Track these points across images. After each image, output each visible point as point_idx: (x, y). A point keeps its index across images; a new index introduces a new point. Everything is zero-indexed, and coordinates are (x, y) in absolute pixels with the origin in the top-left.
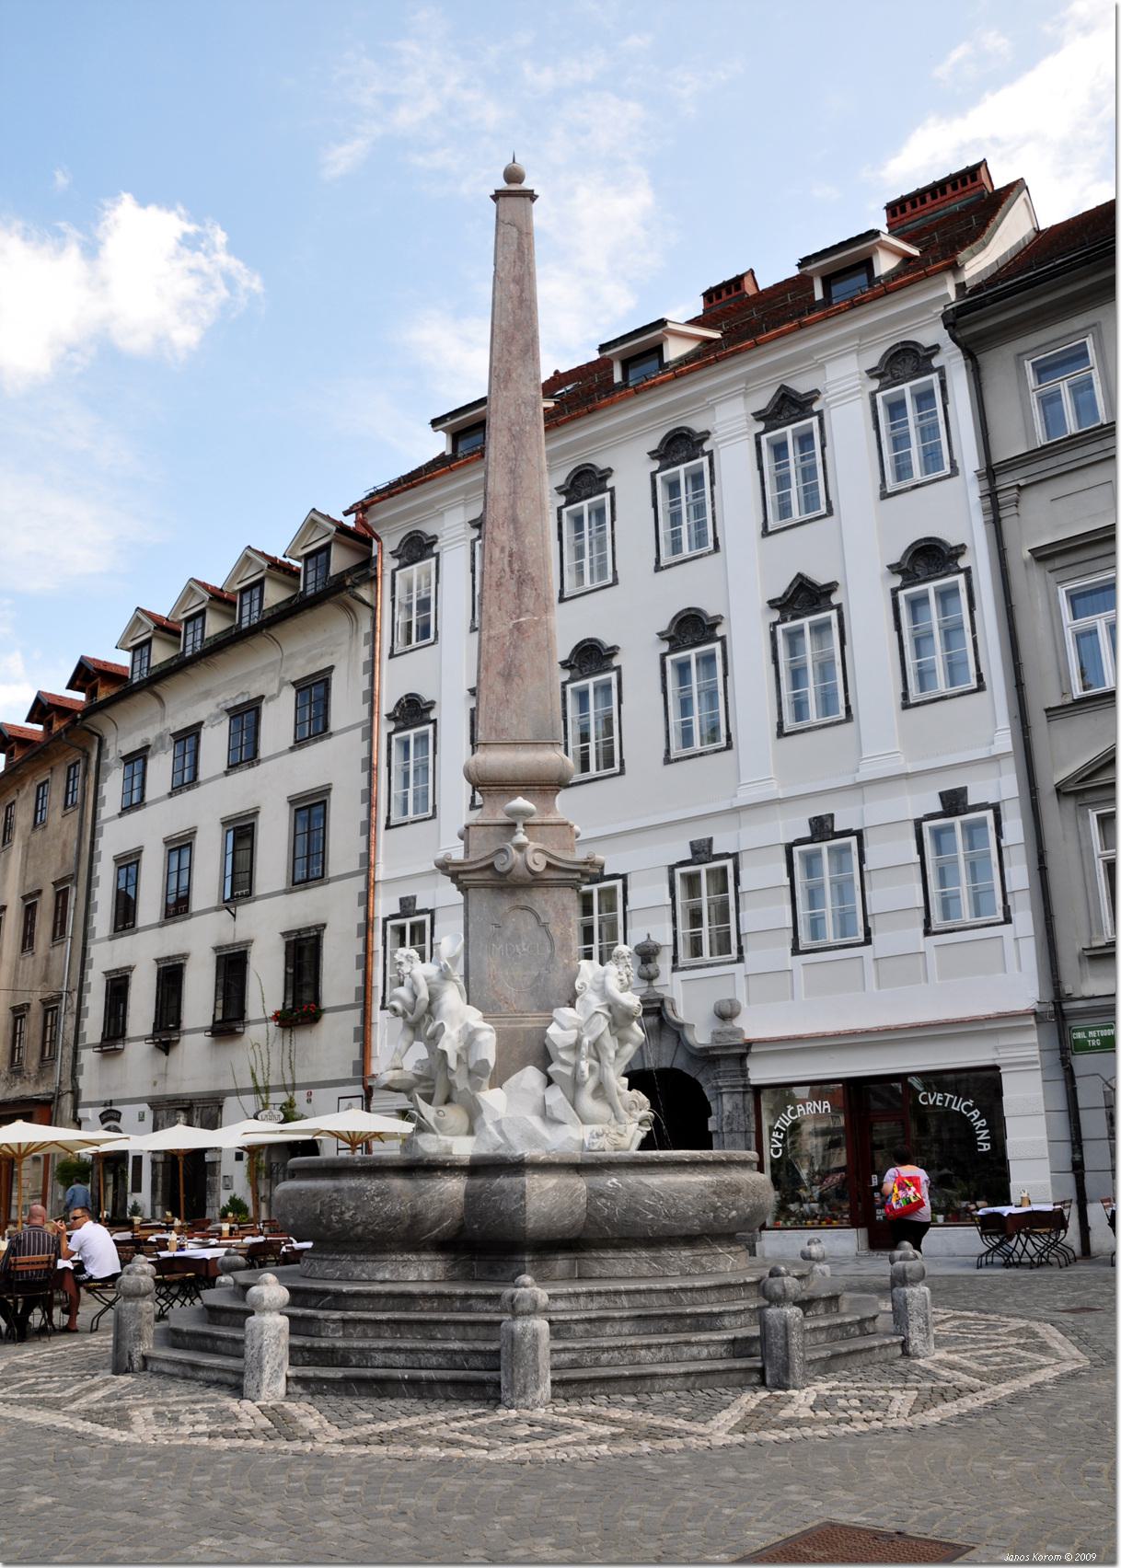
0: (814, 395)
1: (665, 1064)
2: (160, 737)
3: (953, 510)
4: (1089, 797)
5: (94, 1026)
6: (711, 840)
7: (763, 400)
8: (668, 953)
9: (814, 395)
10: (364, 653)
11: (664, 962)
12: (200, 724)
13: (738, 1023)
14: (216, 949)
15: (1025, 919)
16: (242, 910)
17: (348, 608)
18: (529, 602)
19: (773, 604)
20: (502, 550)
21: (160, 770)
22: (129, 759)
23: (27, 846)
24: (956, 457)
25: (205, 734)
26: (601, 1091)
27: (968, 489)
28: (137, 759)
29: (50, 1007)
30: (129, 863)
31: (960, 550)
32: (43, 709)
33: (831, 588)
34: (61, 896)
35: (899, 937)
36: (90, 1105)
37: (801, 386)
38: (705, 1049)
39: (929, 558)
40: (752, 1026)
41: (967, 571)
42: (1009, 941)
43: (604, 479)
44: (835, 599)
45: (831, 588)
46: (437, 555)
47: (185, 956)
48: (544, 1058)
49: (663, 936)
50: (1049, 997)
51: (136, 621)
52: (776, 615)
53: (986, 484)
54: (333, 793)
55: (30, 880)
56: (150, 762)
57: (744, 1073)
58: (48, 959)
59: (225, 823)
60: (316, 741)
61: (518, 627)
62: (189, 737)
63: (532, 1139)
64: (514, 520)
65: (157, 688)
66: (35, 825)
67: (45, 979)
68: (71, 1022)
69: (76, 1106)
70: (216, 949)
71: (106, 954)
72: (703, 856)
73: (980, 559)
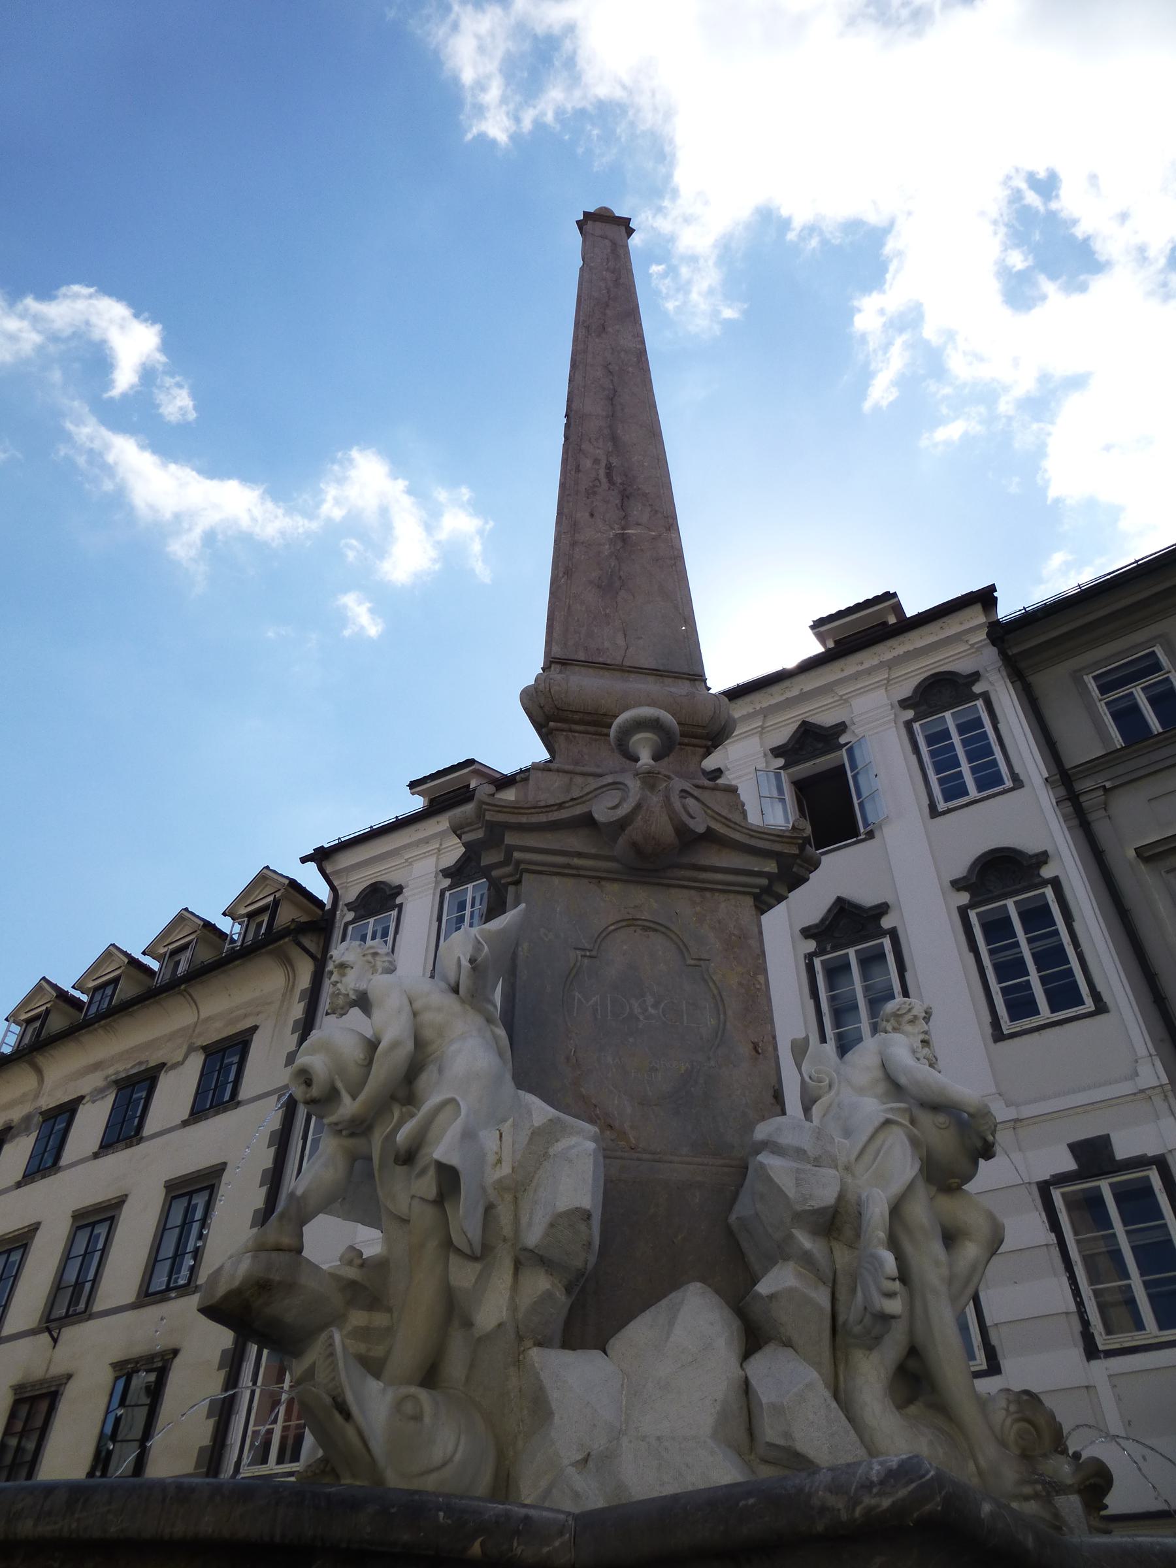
2: (27, 1118)
7: (782, 735)
10: (298, 1010)
12: (82, 1097)
16: (69, 1334)
17: (287, 962)
19: (807, 933)
20: (596, 461)
24: (1017, 770)
31: (1043, 858)
33: (883, 909)
39: (999, 874)
41: (1056, 883)
44: (886, 923)
45: (883, 909)
46: (400, 906)
51: (38, 990)
52: (811, 946)
53: (1062, 792)
54: (226, 1177)
60: (217, 1113)
61: (624, 538)
64: (614, 438)
65: (40, 1060)
73: (1069, 866)
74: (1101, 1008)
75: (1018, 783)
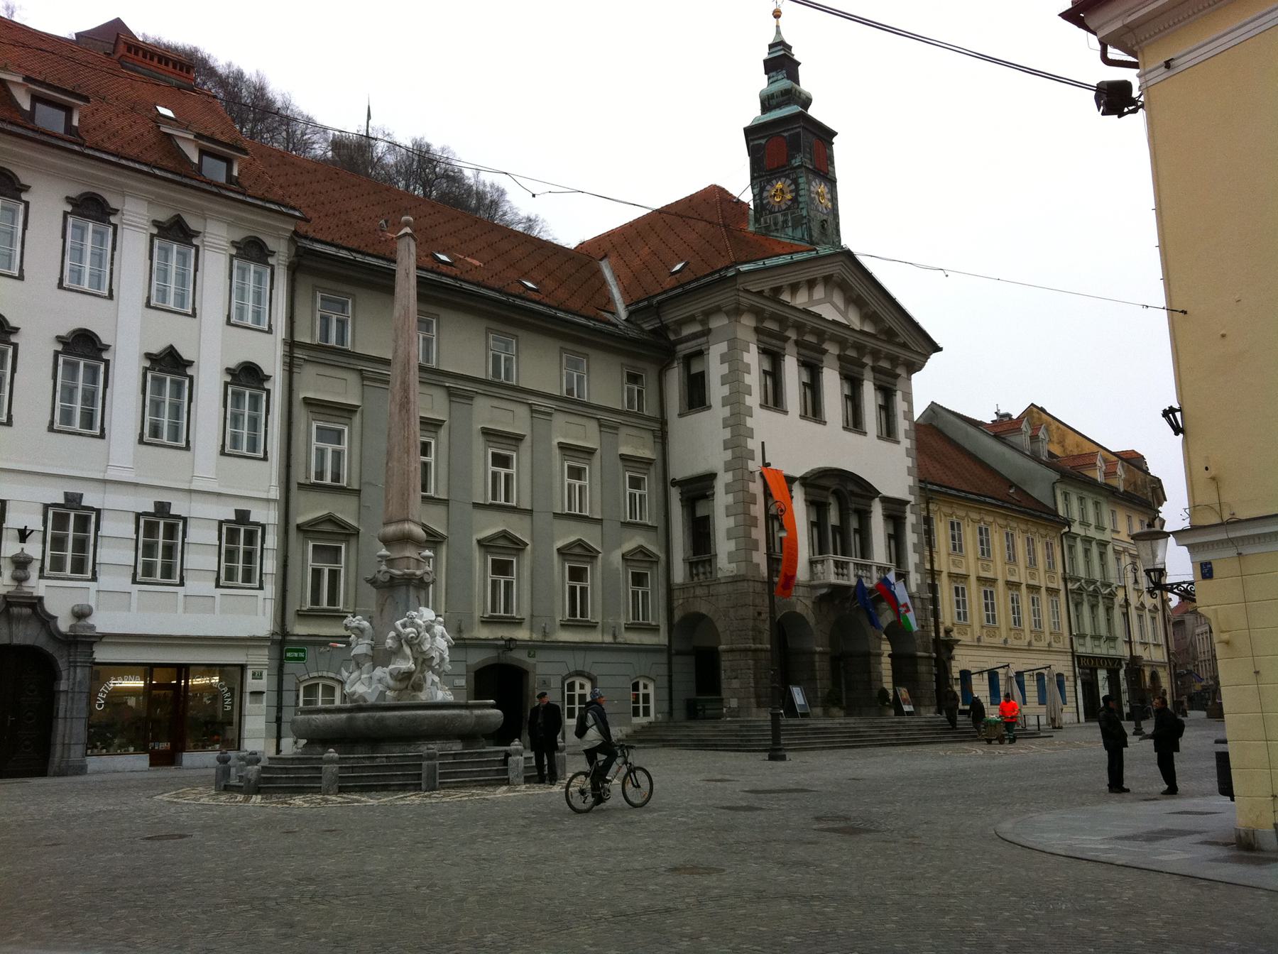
1: (29, 642)
3: (268, 354)
4: (311, 535)
6: (81, 495)
8: (37, 565)
11: (34, 571)
13: (91, 621)
15: (270, 590)
37: (193, 223)
38: (66, 636)
41: (268, 392)
43: (21, 191)
45: (190, 363)
49: (33, 549)
52: (148, 364)
72: (75, 505)
74: (265, 459)
75: (270, 331)
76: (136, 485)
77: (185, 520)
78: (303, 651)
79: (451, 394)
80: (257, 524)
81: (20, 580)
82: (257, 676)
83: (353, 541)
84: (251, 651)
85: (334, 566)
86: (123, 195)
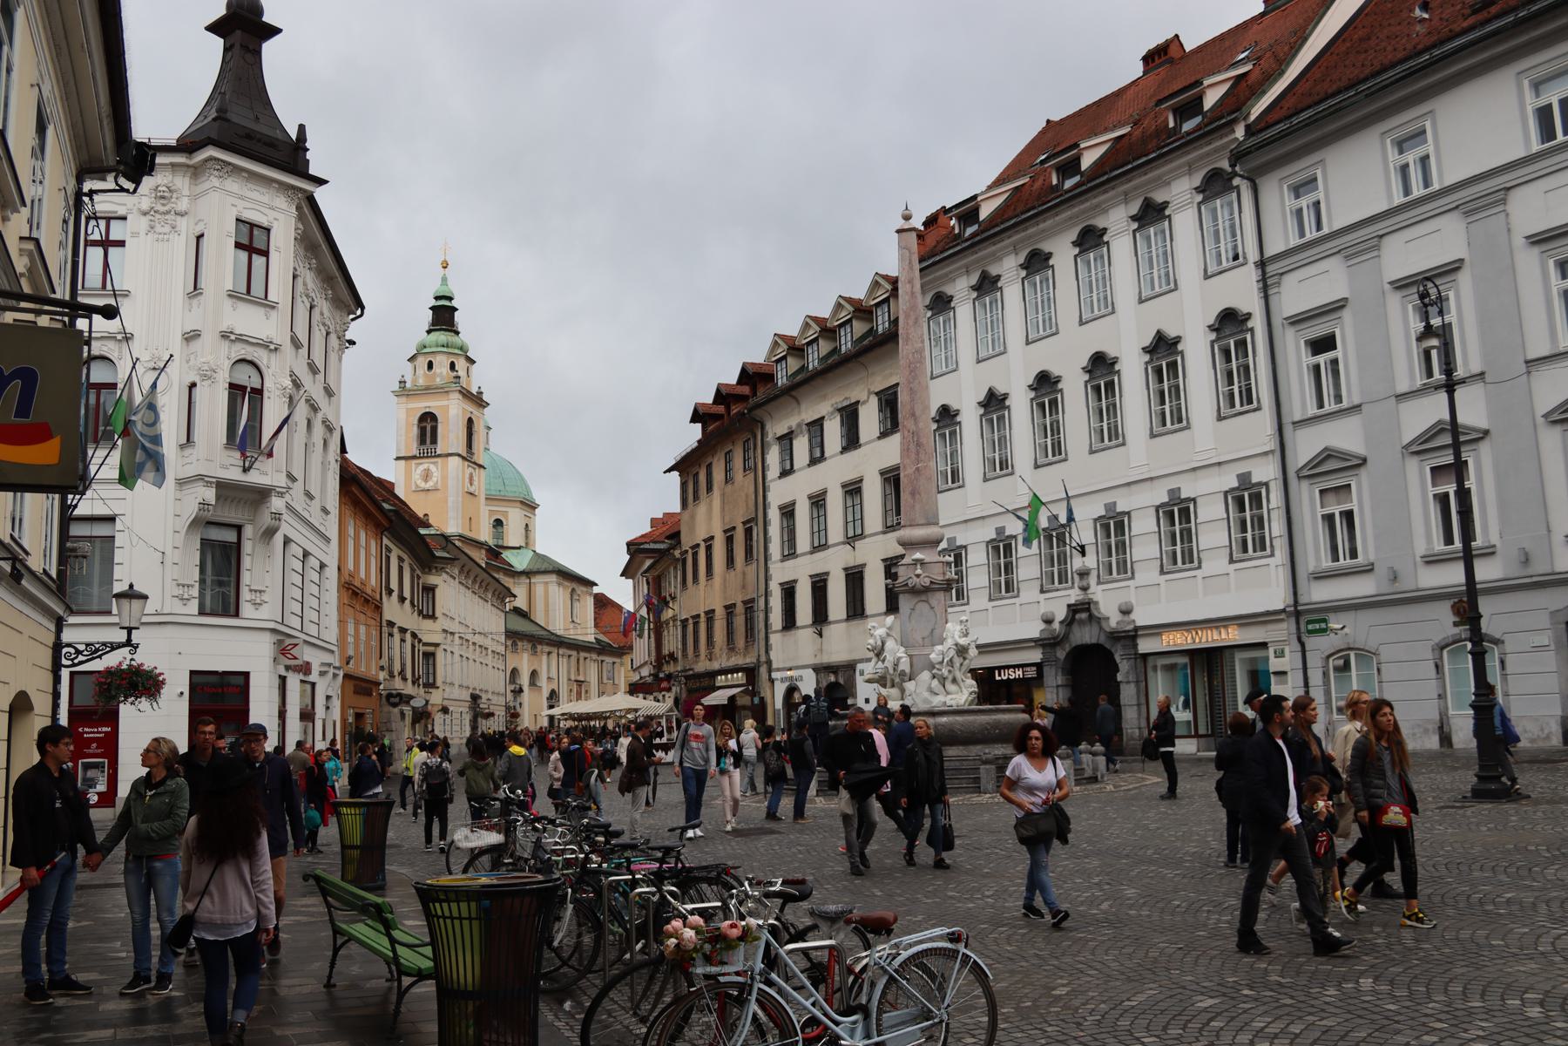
0: (1165, 204)
1: (1094, 641)
2: (799, 425)
5: (776, 619)
7: (1135, 208)
9: (1165, 204)
11: (1093, 580)
13: (1132, 616)
14: (845, 569)
15: (1281, 555)
16: (858, 544)
18: (922, 456)
21: (801, 446)
22: (780, 439)
23: (723, 495)
25: (827, 424)
26: (954, 681)
27: (1248, 276)
28: (787, 439)
29: (749, 605)
30: (788, 512)
31: (1249, 316)
32: (722, 396)
34: (748, 533)
35: (1216, 563)
36: (778, 670)
37: (1159, 197)
40: (1141, 618)
41: (1252, 330)
42: (1272, 567)
47: (827, 574)
48: (932, 666)
49: (1090, 561)
50: (1291, 602)
51: (775, 344)
55: (727, 519)
56: (795, 442)
57: (1135, 646)
58: (744, 574)
59: (844, 486)
62: (817, 426)
63: (926, 701)
64: (913, 415)
66: (727, 482)
67: (744, 587)
68: (762, 615)
69: (770, 671)
70: (845, 569)
71: (780, 572)
73: (1258, 323)
76: (1151, 479)
77: (1194, 500)
78: (1325, 621)
79: (1470, 210)
80: (1260, 484)
81: (1085, 589)
82: (1280, 654)
83: (1363, 472)
84: (1271, 627)
85: (1346, 507)
86: (1105, 211)
